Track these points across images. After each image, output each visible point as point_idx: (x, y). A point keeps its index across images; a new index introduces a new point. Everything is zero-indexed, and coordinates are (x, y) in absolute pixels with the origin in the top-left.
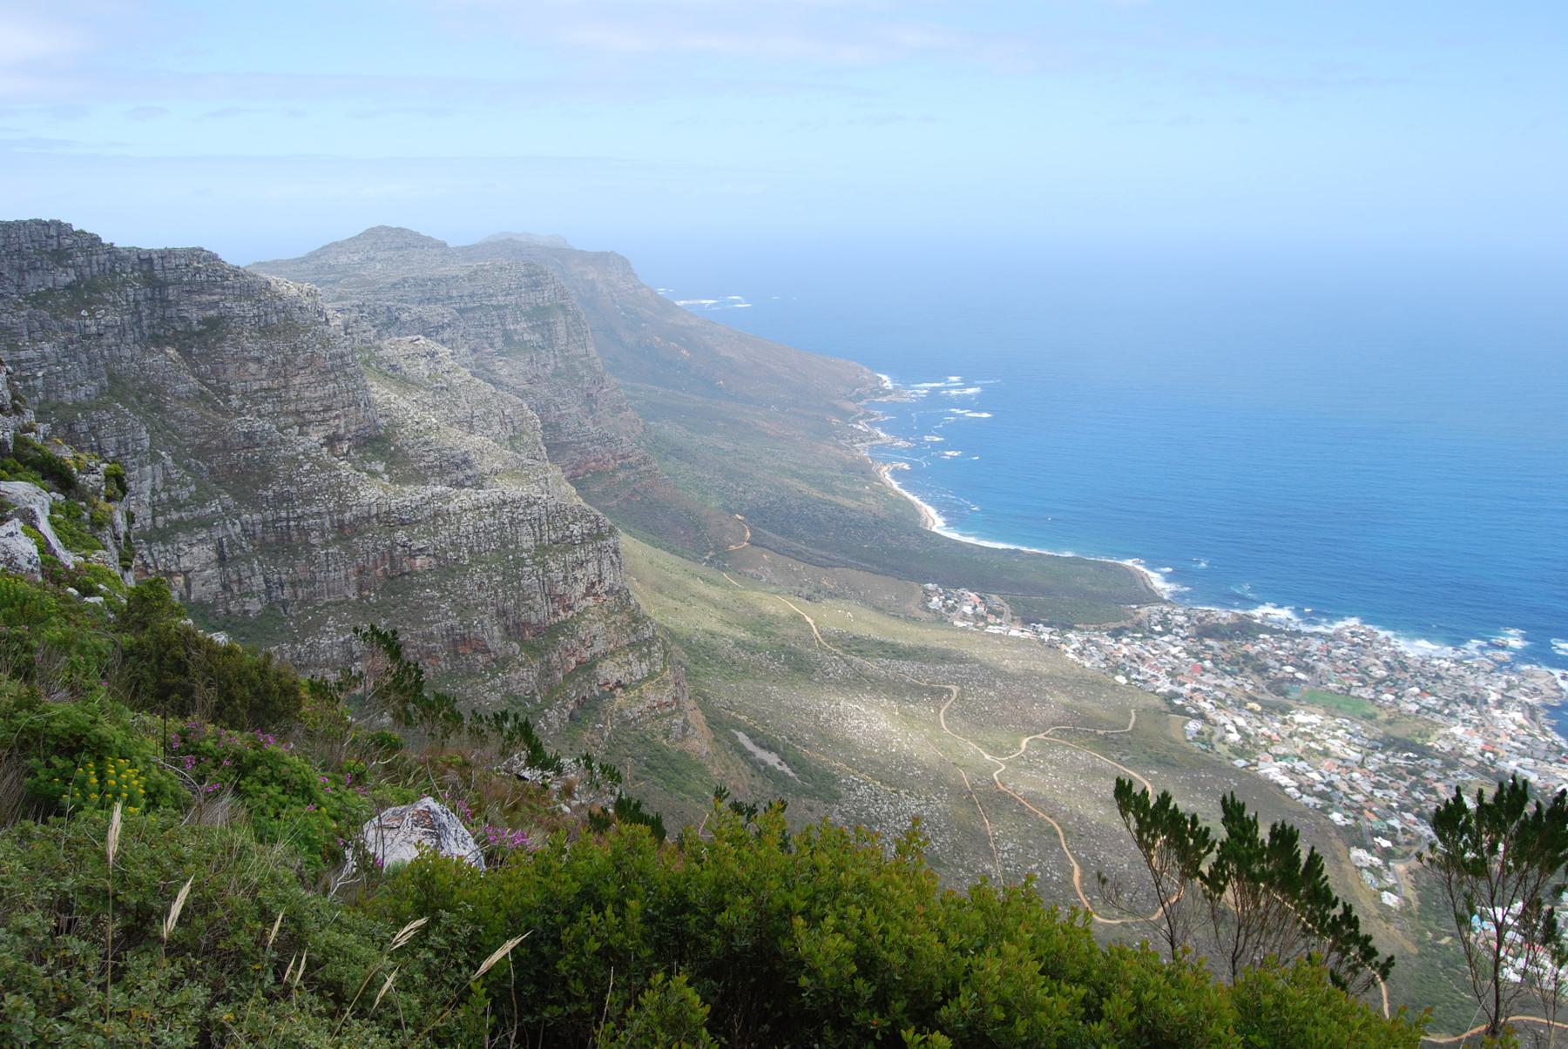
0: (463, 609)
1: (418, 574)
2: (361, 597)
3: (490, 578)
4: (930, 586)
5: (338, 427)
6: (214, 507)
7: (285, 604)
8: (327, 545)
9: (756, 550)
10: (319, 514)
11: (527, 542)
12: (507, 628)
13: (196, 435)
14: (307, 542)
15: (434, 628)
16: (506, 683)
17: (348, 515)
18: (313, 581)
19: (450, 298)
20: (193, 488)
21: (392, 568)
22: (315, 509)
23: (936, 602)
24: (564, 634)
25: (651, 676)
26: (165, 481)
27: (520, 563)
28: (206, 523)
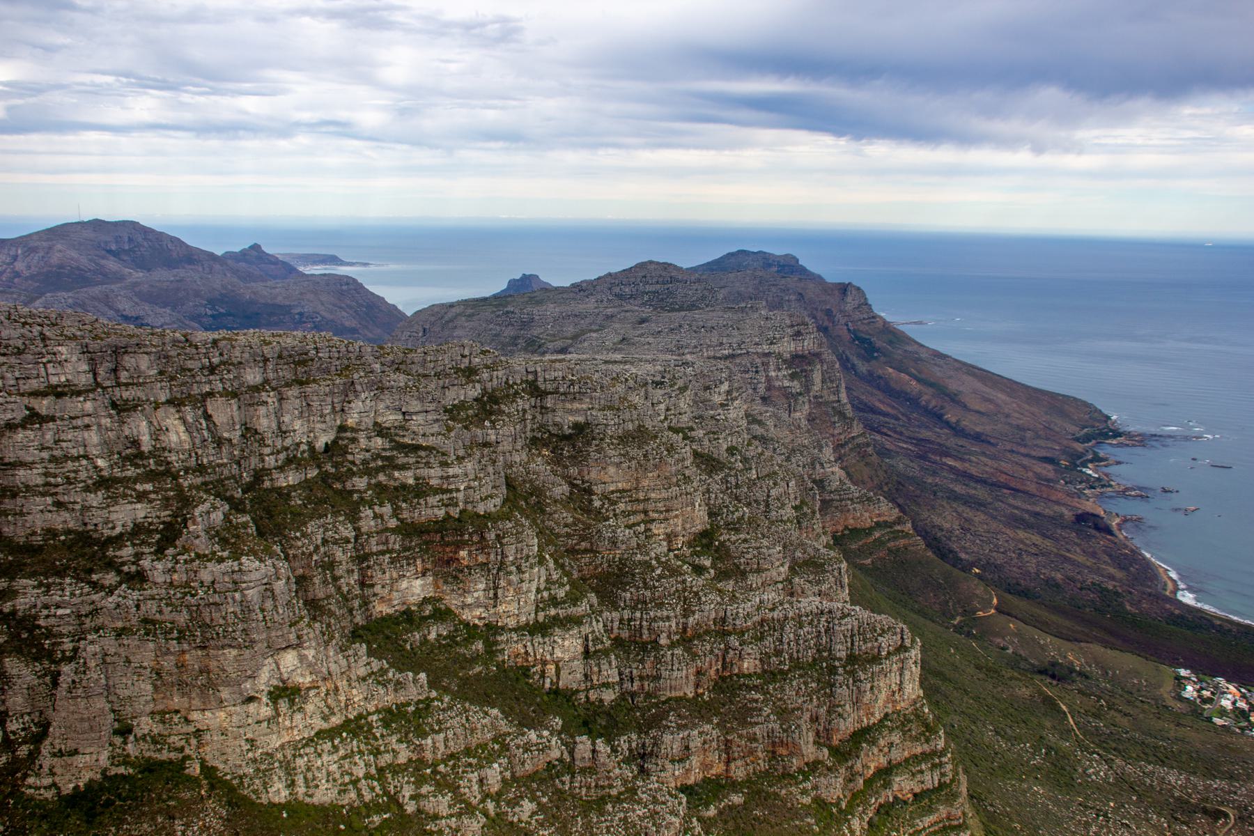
0: (783, 713)
1: (744, 676)
2: (697, 695)
3: (806, 683)
4: (1183, 672)
5: (676, 525)
6: (582, 608)
7: (633, 695)
8: (672, 646)
9: (1003, 618)
10: (668, 618)
11: (841, 652)
12: (818, 733)
13: (568, 535)
14: (656, 641)
15: (757, 729)
16: (815, 788)
17: (691, 619)
18: (658, 678)
19: (721, 344)
20: (568, 587)
21: (724, 668)
22: (665, 613)
23: (1190, 691)
24: (866, 741)
25: (942, 785)
26: (547, 581)
27: (832, 670)
28: (578, 621)
